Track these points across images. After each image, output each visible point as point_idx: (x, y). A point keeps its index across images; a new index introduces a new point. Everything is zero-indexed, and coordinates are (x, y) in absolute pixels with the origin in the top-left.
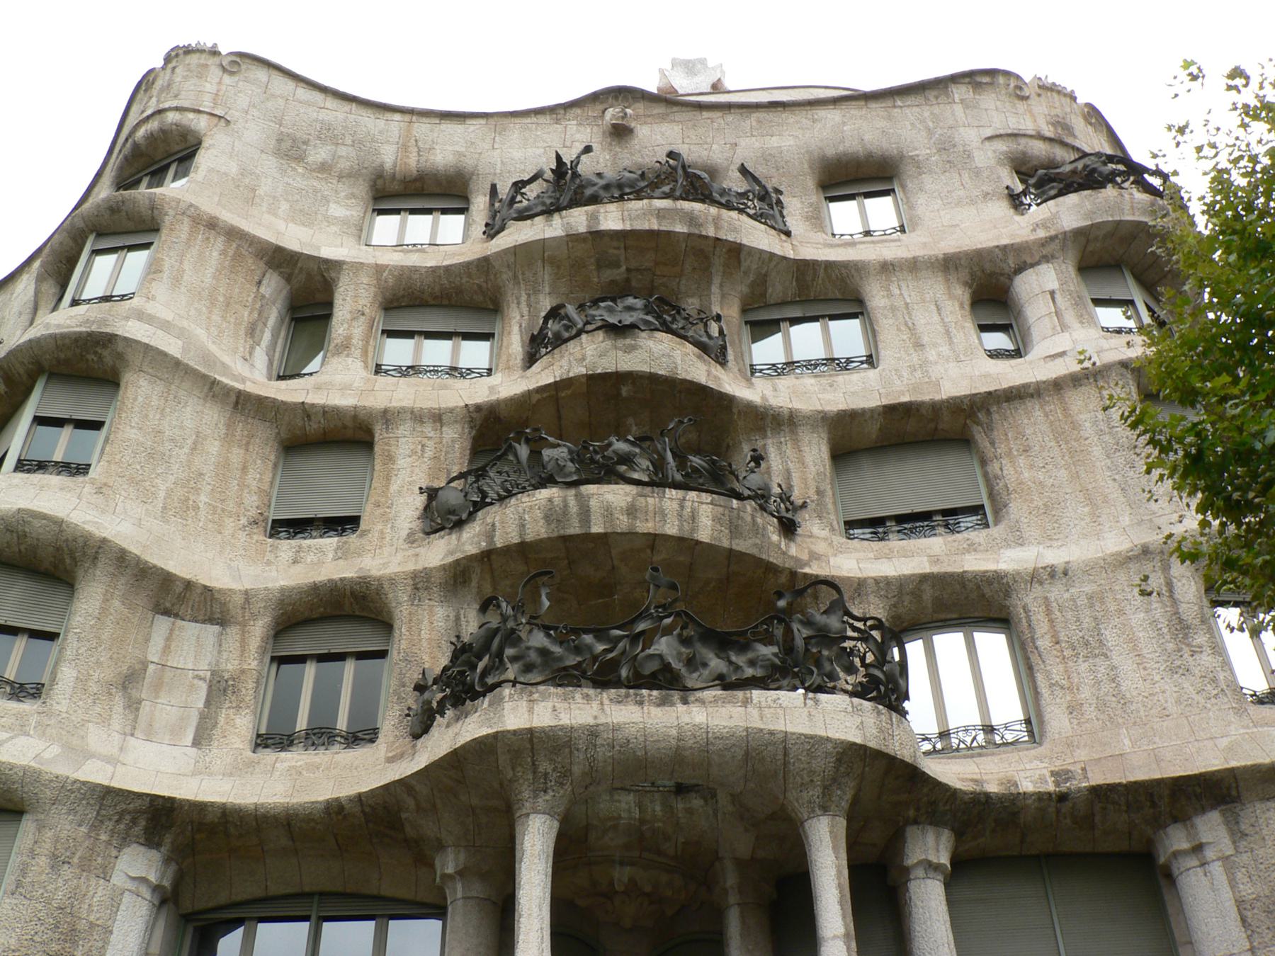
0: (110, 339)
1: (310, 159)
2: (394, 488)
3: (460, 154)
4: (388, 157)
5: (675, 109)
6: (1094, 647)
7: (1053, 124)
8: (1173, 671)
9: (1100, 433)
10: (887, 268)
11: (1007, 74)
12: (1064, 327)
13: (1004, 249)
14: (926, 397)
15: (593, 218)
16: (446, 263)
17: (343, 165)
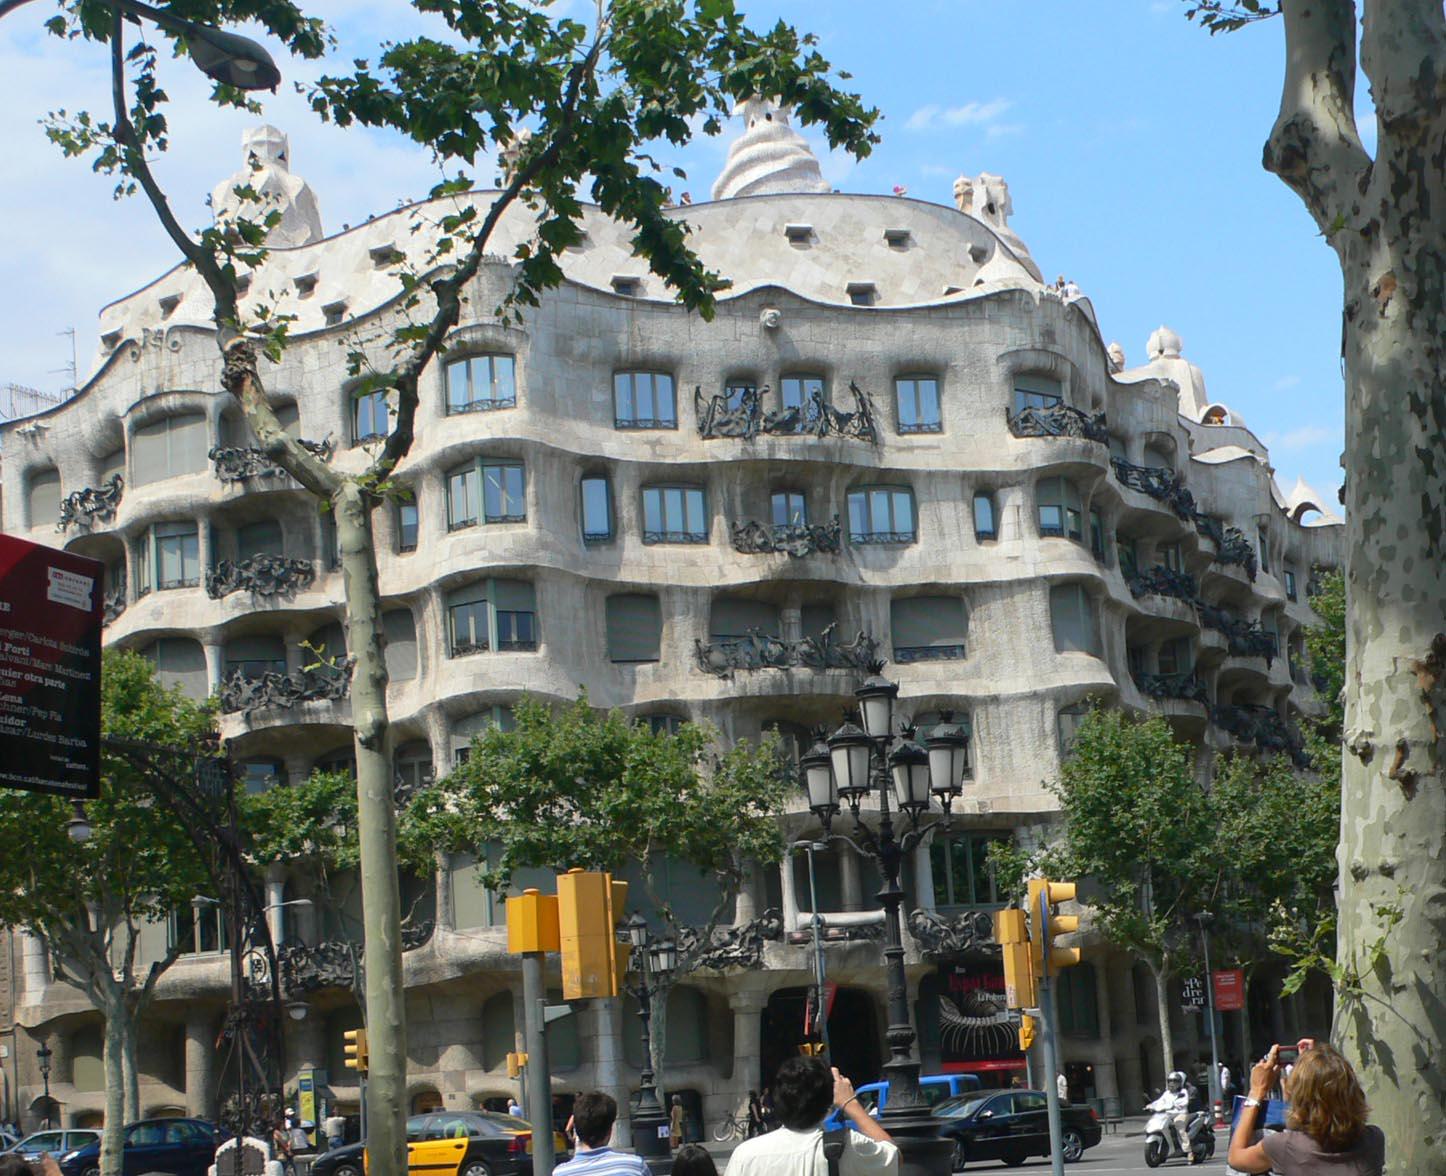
0: (534, 567)
1: (575, 352)
2: (676, 635)
3: (667, 343)
4: (623, 343)
5: (806, 305)
6: (1005, 740)
7: (1041, 334)
8: (1036, 756)
9: (1026, 616)
10: (930, 474)
11: (1022, 291)
12: (1021, 537)
13: (997, 472)
14: (942, 581)
15: (772, 447)
16: (681, 460)
17: (595, 353)
